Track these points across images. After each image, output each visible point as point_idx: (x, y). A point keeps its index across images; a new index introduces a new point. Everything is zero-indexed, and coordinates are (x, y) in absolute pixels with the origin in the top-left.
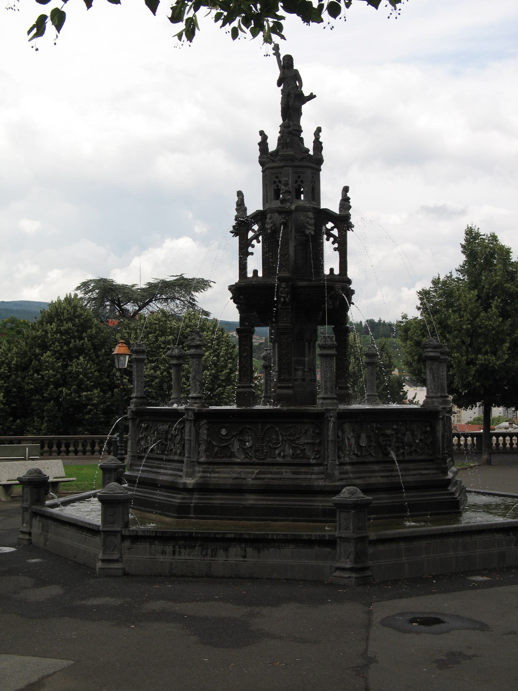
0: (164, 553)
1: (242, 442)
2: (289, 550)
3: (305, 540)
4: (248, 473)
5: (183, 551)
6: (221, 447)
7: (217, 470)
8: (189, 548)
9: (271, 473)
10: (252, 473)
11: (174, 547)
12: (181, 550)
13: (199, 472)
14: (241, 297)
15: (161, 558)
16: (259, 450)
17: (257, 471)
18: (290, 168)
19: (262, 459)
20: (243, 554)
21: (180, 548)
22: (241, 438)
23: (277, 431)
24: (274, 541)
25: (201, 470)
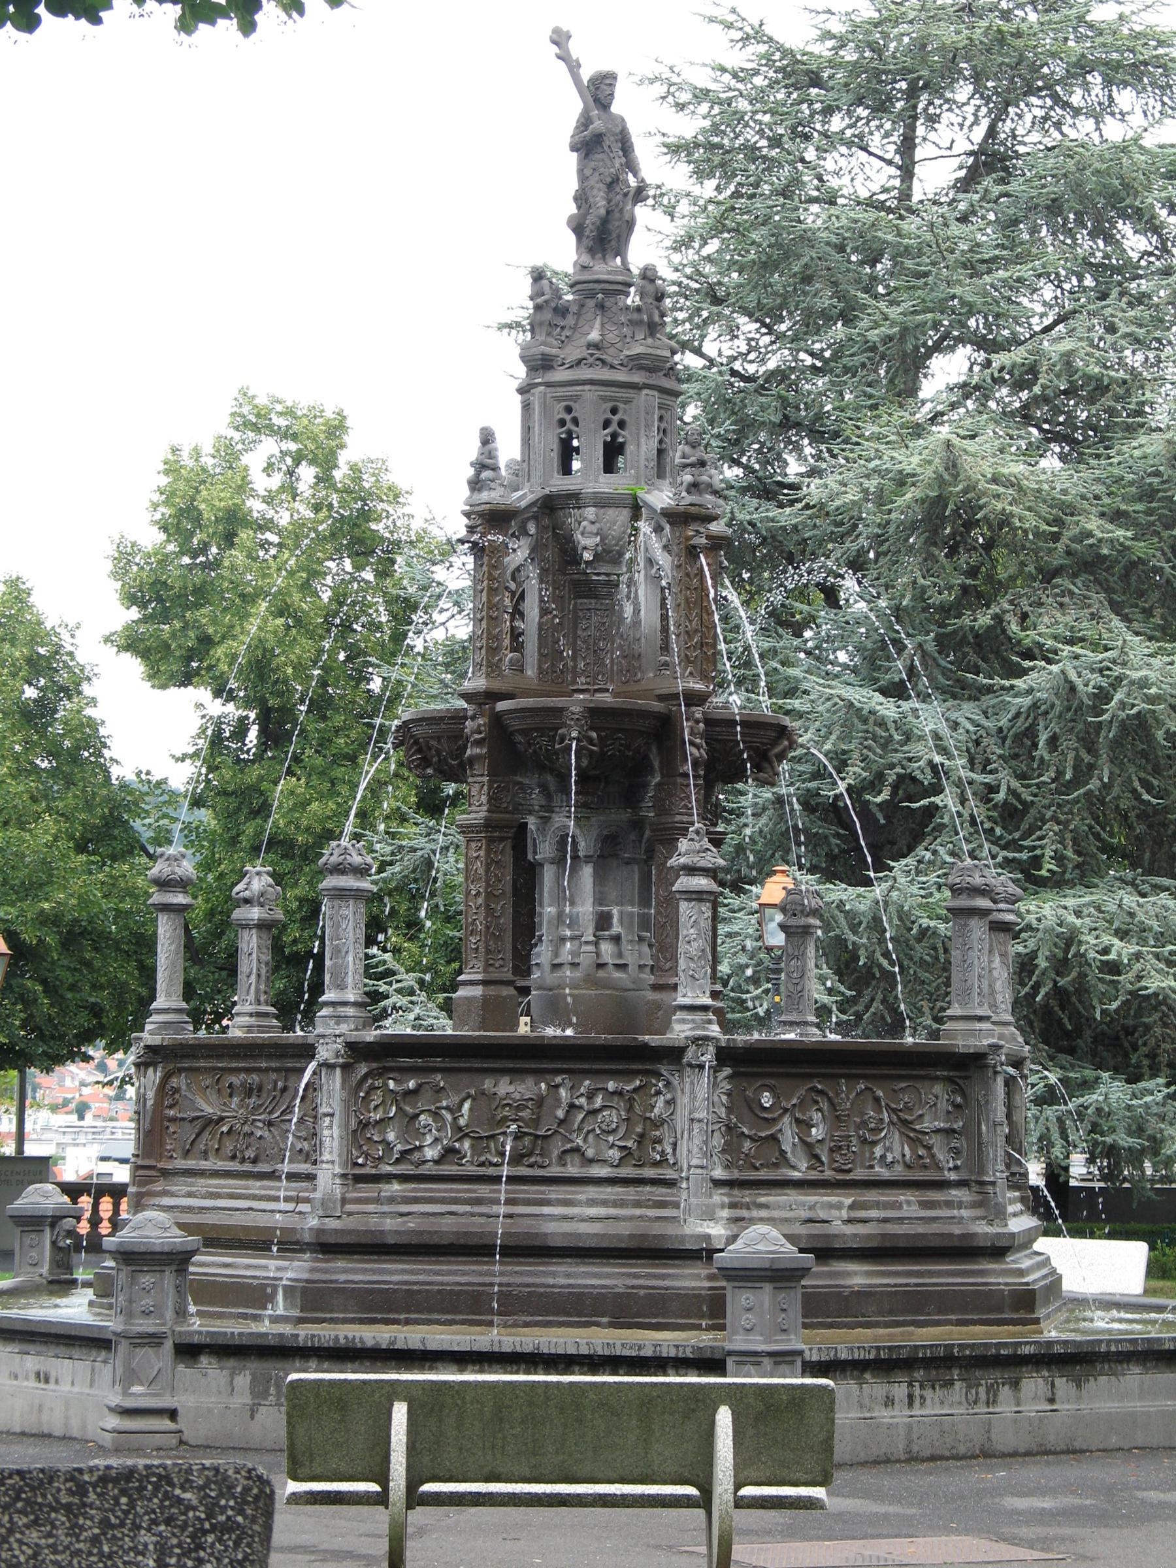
0: (889, 1402)
1: (804, 1125)
2: (1134, 1377)
3: (1168, 1351)
4: (831, 1206)
5: (928, 1393)
6: (762, 1138)
7: (763, 1200)
8: (941, 1386)
9: (877, 1205)
10: (839, 1206)
11: (910, 1385)
12: (925, 1393)
13: (723, 1206)
14: (594, 735)
15: (884, 1415)
16: (840, 1148)
17: (849, 1201)
18: (656, 393)
19: (849, 1171)
20: (1049, 1395)
21: (922, 1387)
22: (801, 1117)
23: (877, 1100)
24: (1107, 1357)
25: (726, 1200)
